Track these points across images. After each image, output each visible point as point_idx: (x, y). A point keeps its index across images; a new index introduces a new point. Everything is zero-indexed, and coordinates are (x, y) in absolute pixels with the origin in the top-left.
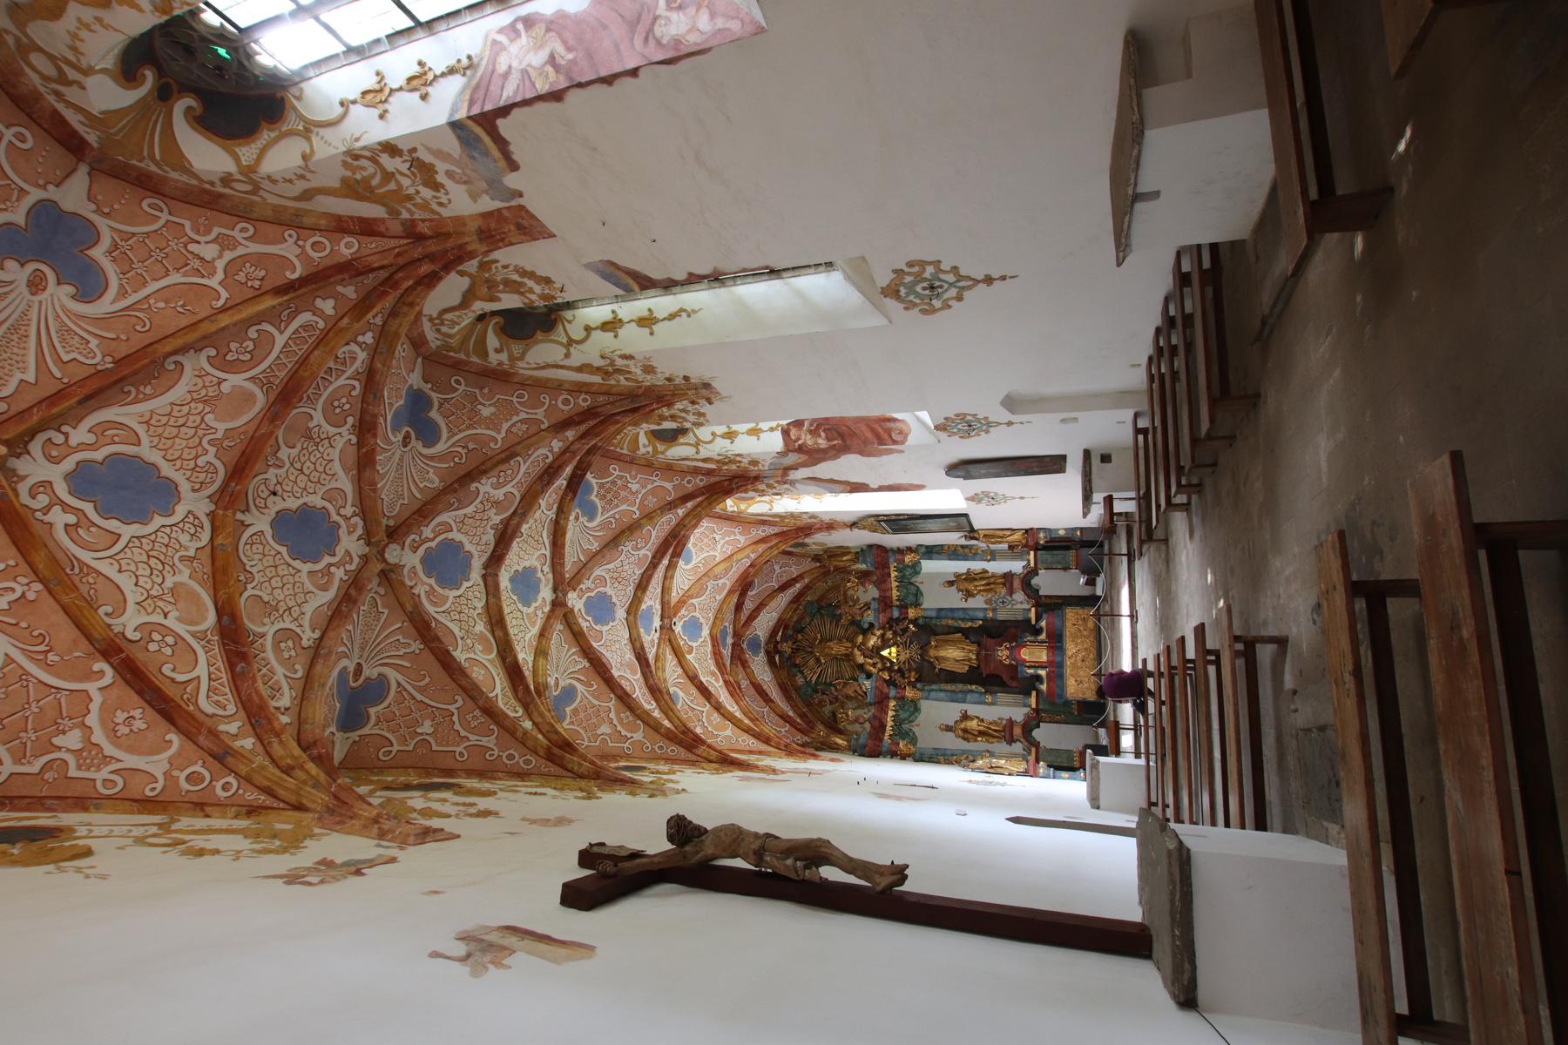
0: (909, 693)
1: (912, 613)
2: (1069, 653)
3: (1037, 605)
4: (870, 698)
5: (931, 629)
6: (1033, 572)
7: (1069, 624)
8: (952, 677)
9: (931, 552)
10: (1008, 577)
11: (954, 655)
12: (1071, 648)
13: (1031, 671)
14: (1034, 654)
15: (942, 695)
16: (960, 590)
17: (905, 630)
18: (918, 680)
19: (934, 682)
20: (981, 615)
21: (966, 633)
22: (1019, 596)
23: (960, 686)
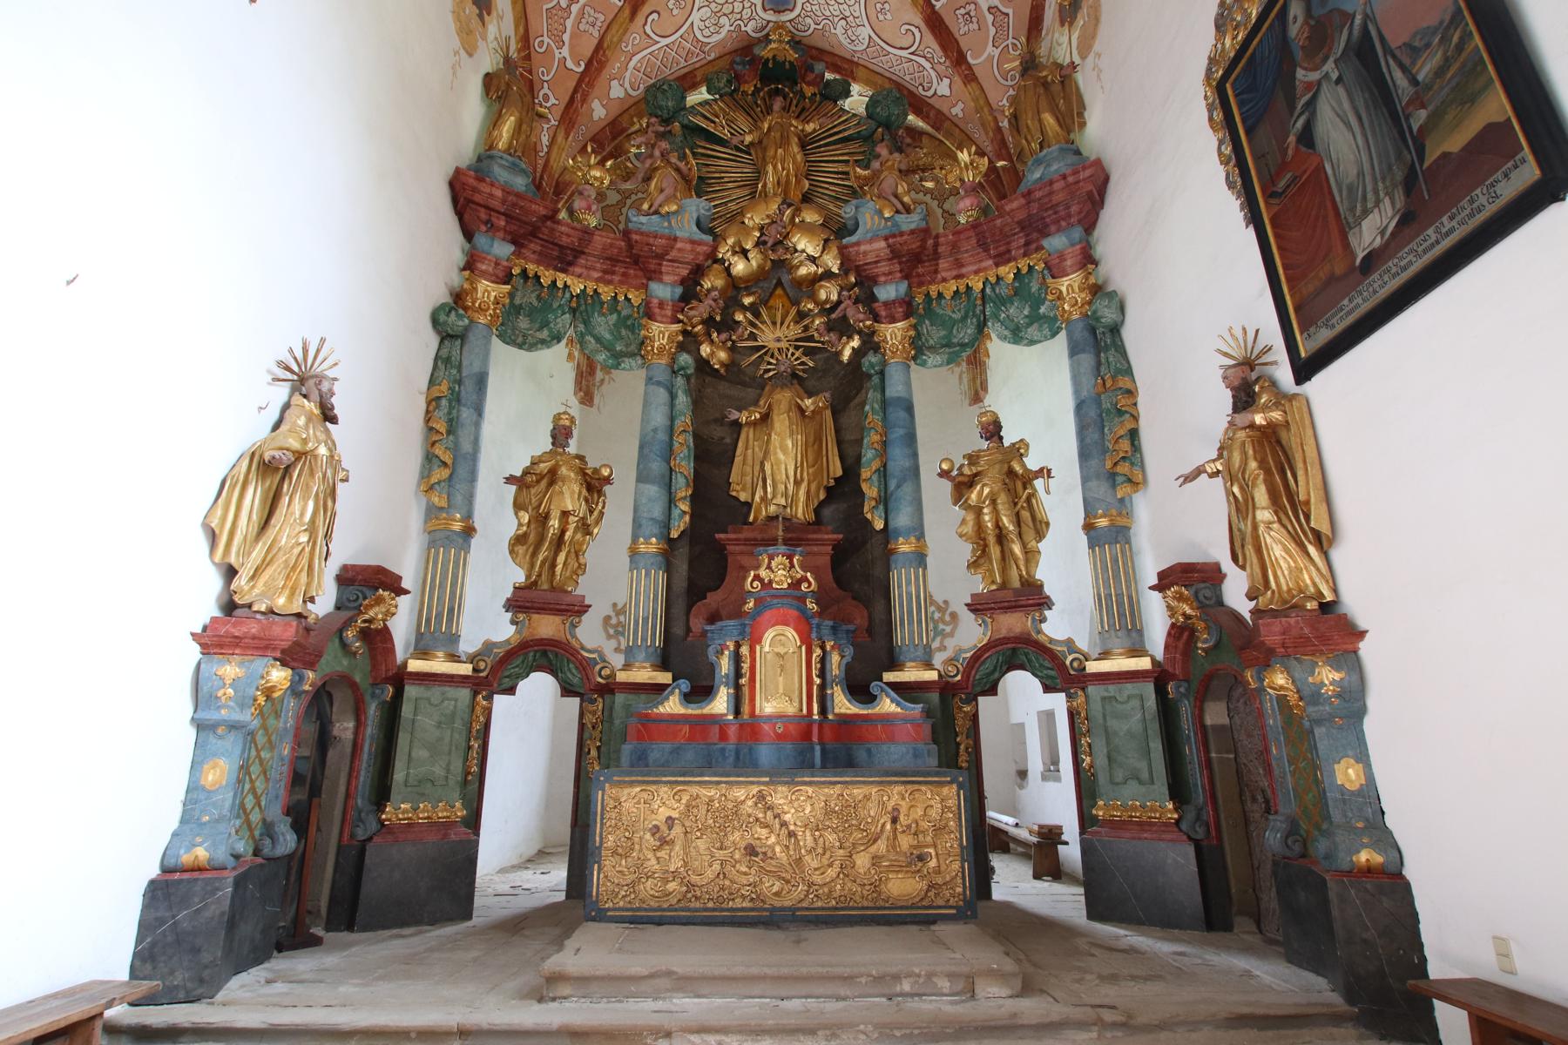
0: (661, 333)
1: (893, 333)
2: (780, 796)
3: (945, 688)
4: (642, 222)
5: (846, 393)
6: (1060, 673)
7: (895, 795)
8: (713, 457)
9: (1101, 344)
10: (1034, 598)
11: (779, 466)
12: (801, 803)
13: (725, 665)
14: (779, 671)
15: (659, 418)
16: (973, 459)
17: (843, 328)
18: (703, 365)
19: (697, 403)
20: (902, 519)
21: (844, 490)
22: (971, 634)
23: (685, 465)
